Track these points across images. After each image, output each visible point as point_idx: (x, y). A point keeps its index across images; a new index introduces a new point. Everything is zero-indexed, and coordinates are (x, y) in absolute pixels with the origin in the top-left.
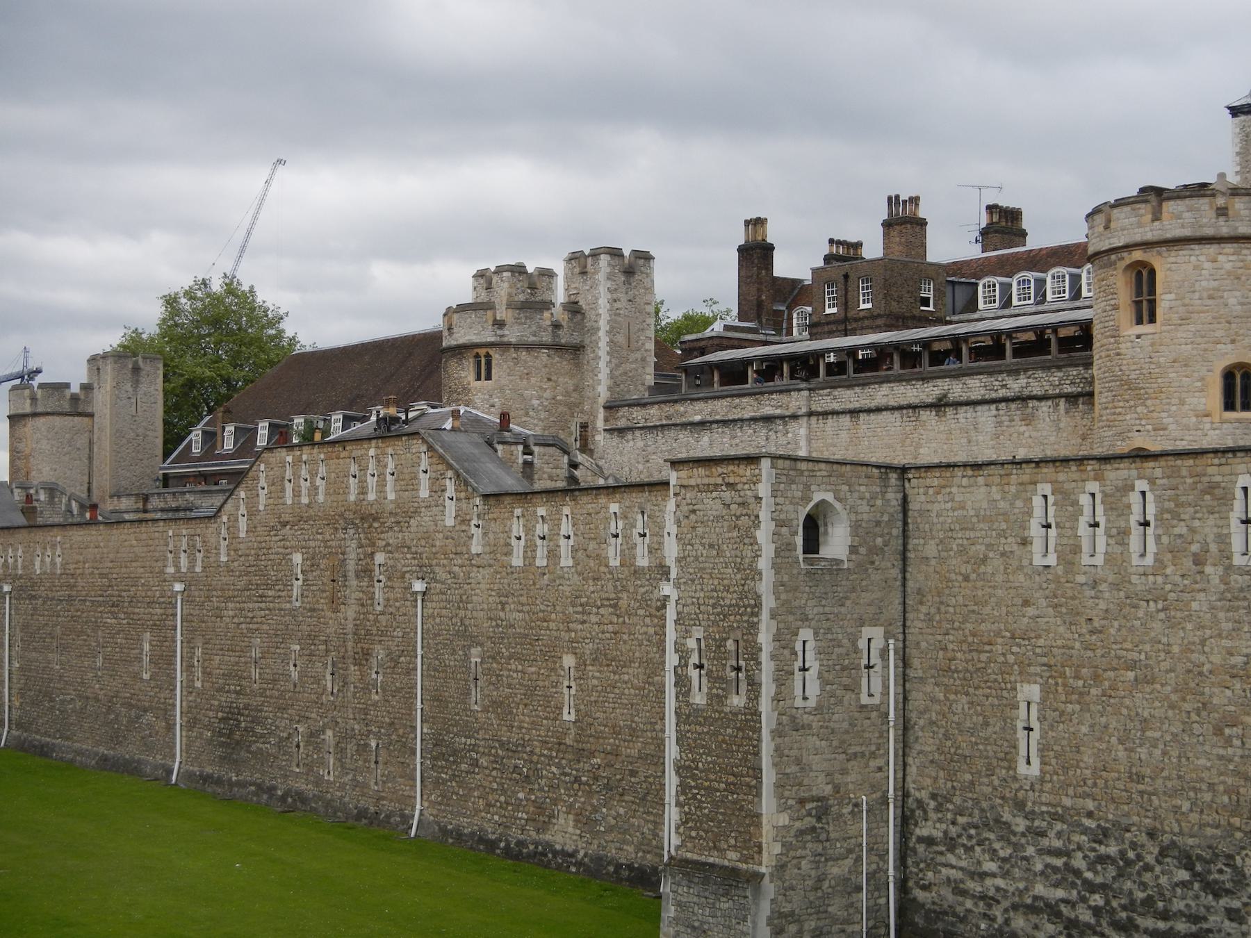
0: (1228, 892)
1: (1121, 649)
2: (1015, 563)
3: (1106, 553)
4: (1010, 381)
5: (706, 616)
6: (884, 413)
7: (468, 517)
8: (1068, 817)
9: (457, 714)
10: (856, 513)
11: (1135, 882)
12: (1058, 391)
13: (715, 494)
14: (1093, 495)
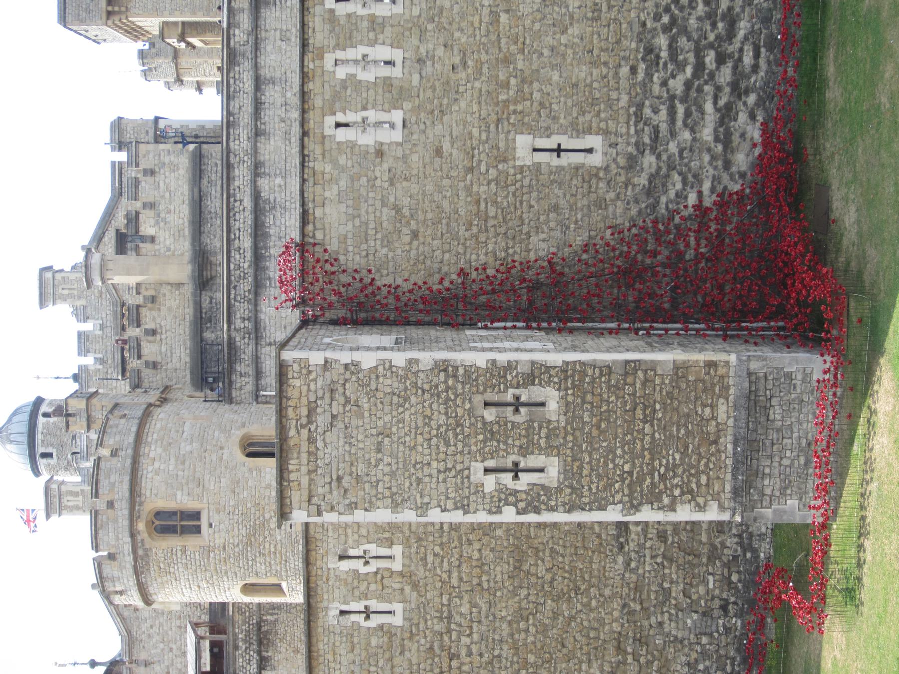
1: (480, 29)
2: (400, 166)
3: (392, 46)
5: (459, 458)
8: (638, 99)
11: (690, 14)
13: (320, 444)
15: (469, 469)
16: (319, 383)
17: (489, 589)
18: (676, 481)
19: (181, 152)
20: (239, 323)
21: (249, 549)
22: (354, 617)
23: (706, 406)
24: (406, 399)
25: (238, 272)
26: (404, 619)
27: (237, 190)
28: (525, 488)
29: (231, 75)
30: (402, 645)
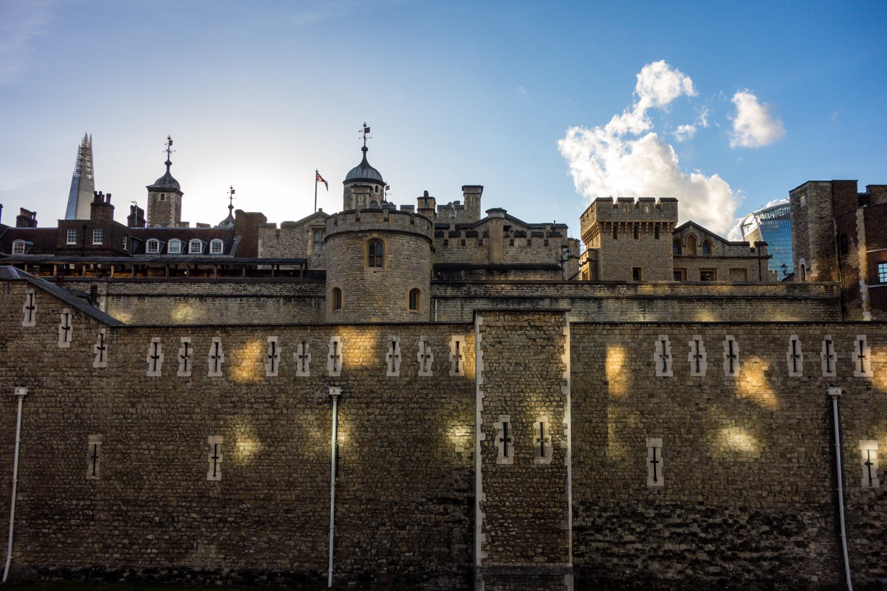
0: (796, 533)
3: (707, 371)
4: (249, 288)
5: (513, 408)
7: (89, 342)
8: (685, 506)
9: (69, 483)
11: (734, 535)
13: (519, 332)
14: (697, 342)
15: (507, 414)
16: (553, 332)
17: (407, 425)
18: (500, 532)
20: (473, 289)
22: (391, 349)
23: (543, 550)
24: (545, 379)
26: (390, 377)
28: (496, 445)
30: (374, 376)
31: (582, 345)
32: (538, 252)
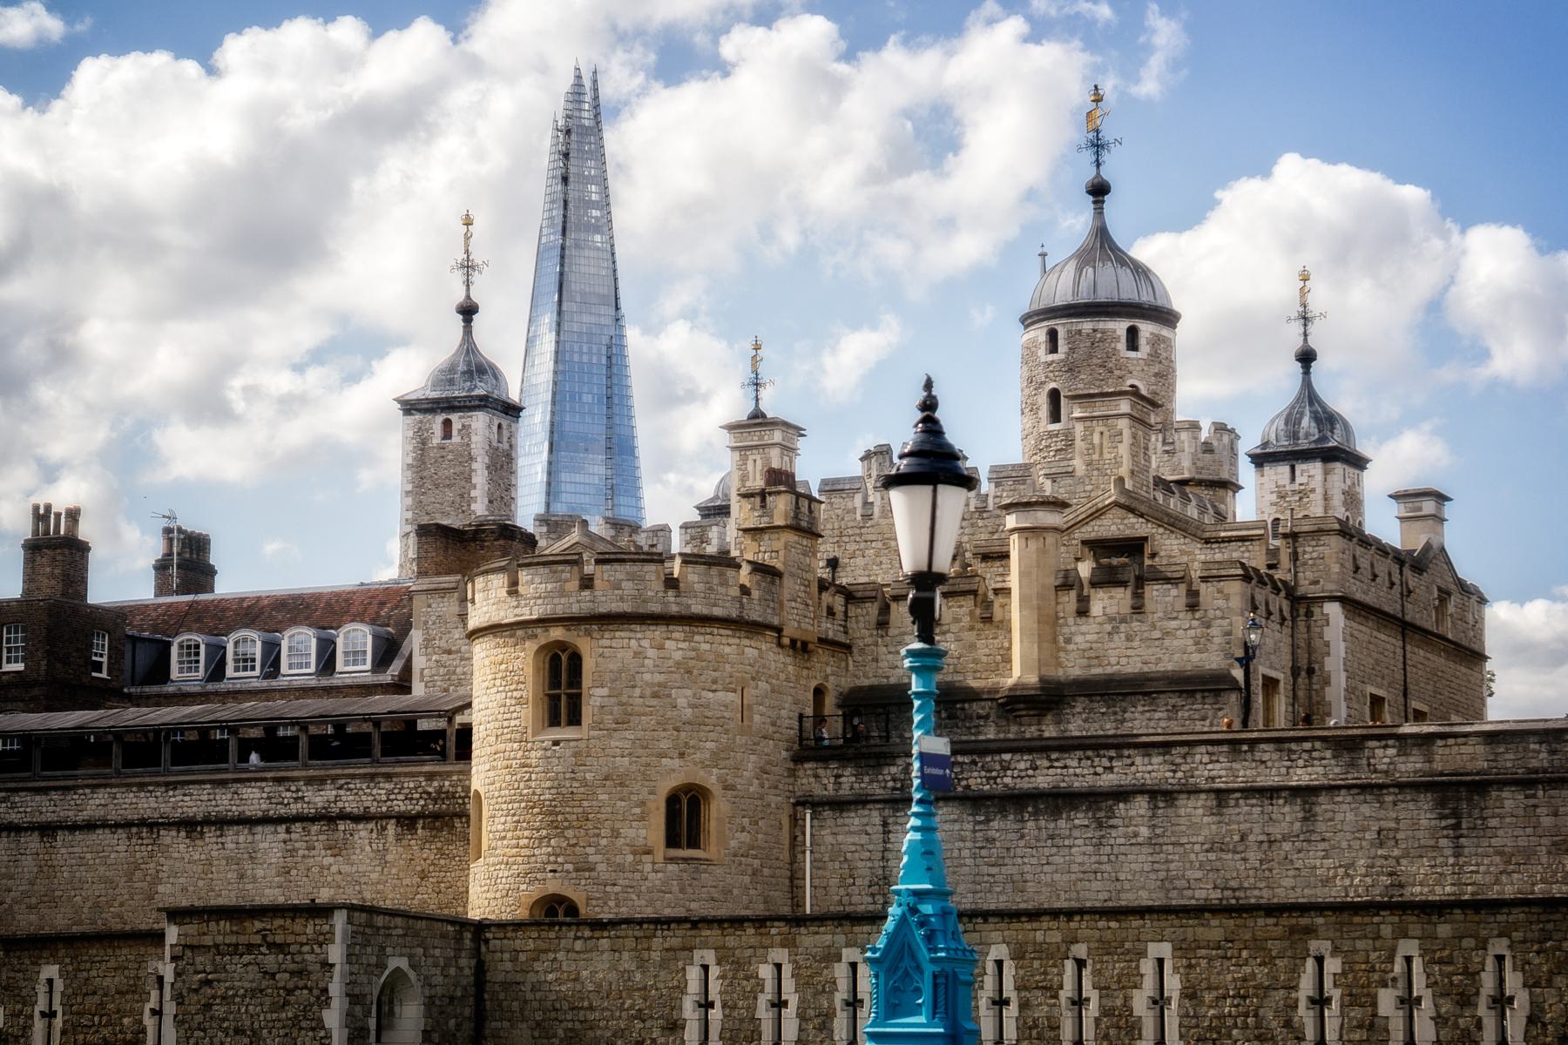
4: (309, 793)
6: (100, 831)
10: (430, 985)
12: (384, 809)
13: (246, 959)
14: (778, 966)
19: (1229, 655)
21: (523, 805)
22: (154, 994)
25: (998, 767)
27: (1129, 761)
29: (1318, 745)
31: (531, 977)
32: (1167, 633)
